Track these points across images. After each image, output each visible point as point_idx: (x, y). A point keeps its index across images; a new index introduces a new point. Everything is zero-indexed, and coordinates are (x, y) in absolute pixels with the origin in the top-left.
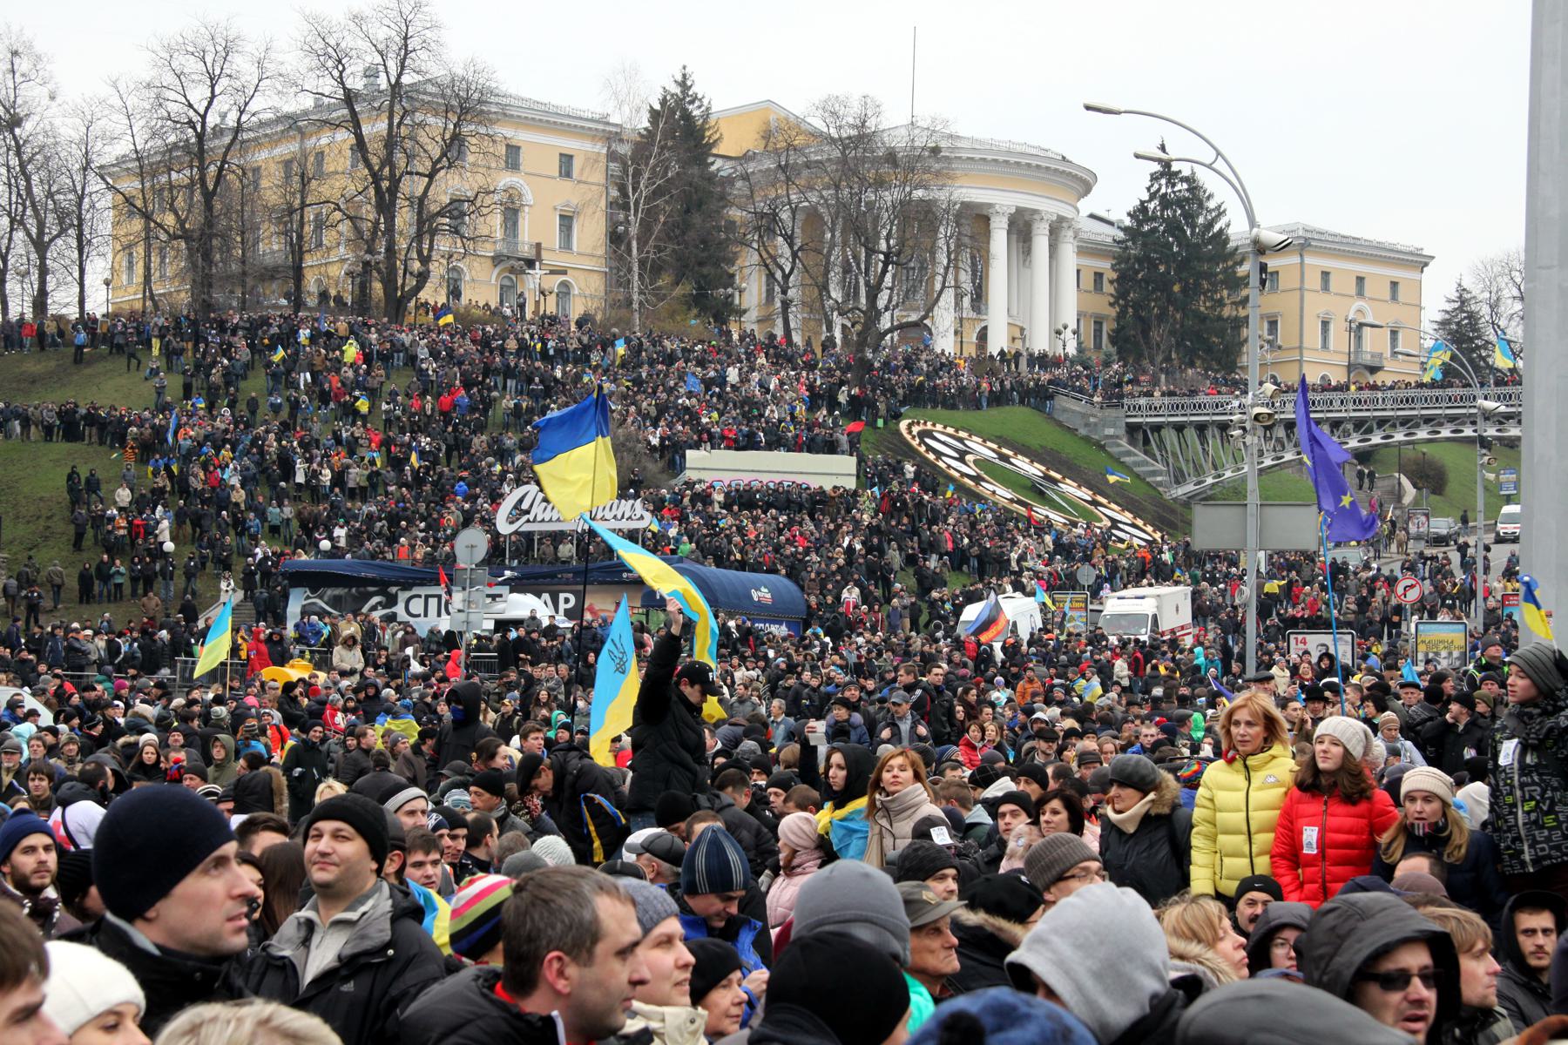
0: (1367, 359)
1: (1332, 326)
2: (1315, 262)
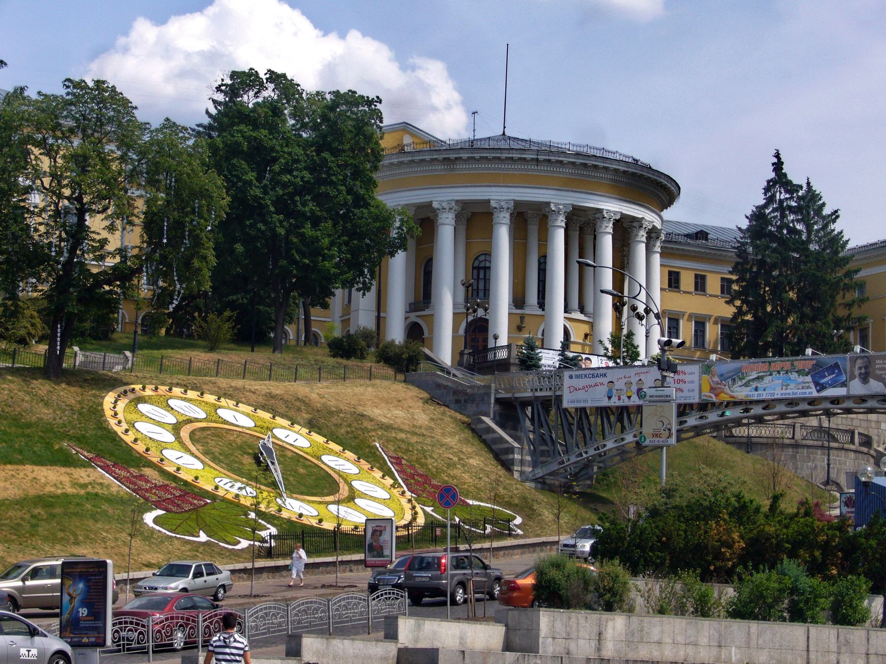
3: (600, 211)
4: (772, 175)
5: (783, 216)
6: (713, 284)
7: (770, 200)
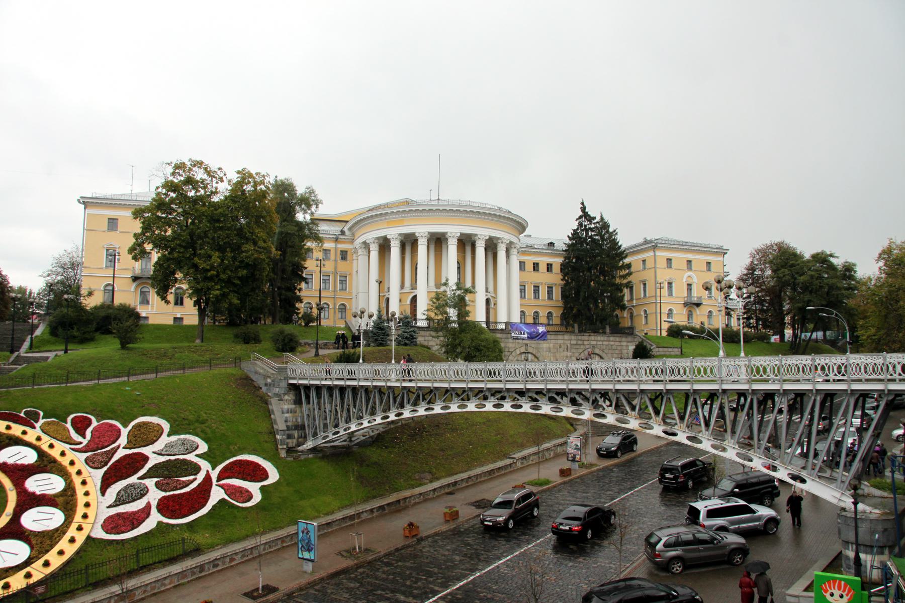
0: (695, 300)
1: (674, 285)
2: (662, 254)
3: (476, 235)
4: (581, 213)
5: (587, 234)
6: (556, 268)
7: (580, 225)
